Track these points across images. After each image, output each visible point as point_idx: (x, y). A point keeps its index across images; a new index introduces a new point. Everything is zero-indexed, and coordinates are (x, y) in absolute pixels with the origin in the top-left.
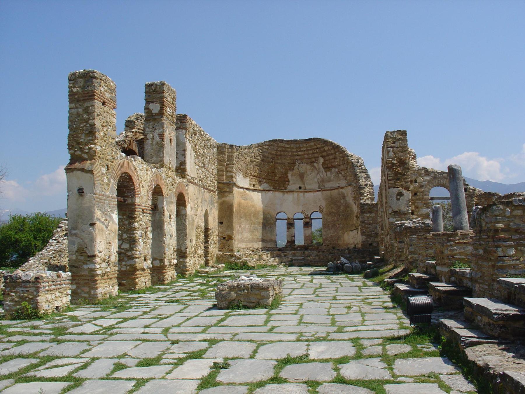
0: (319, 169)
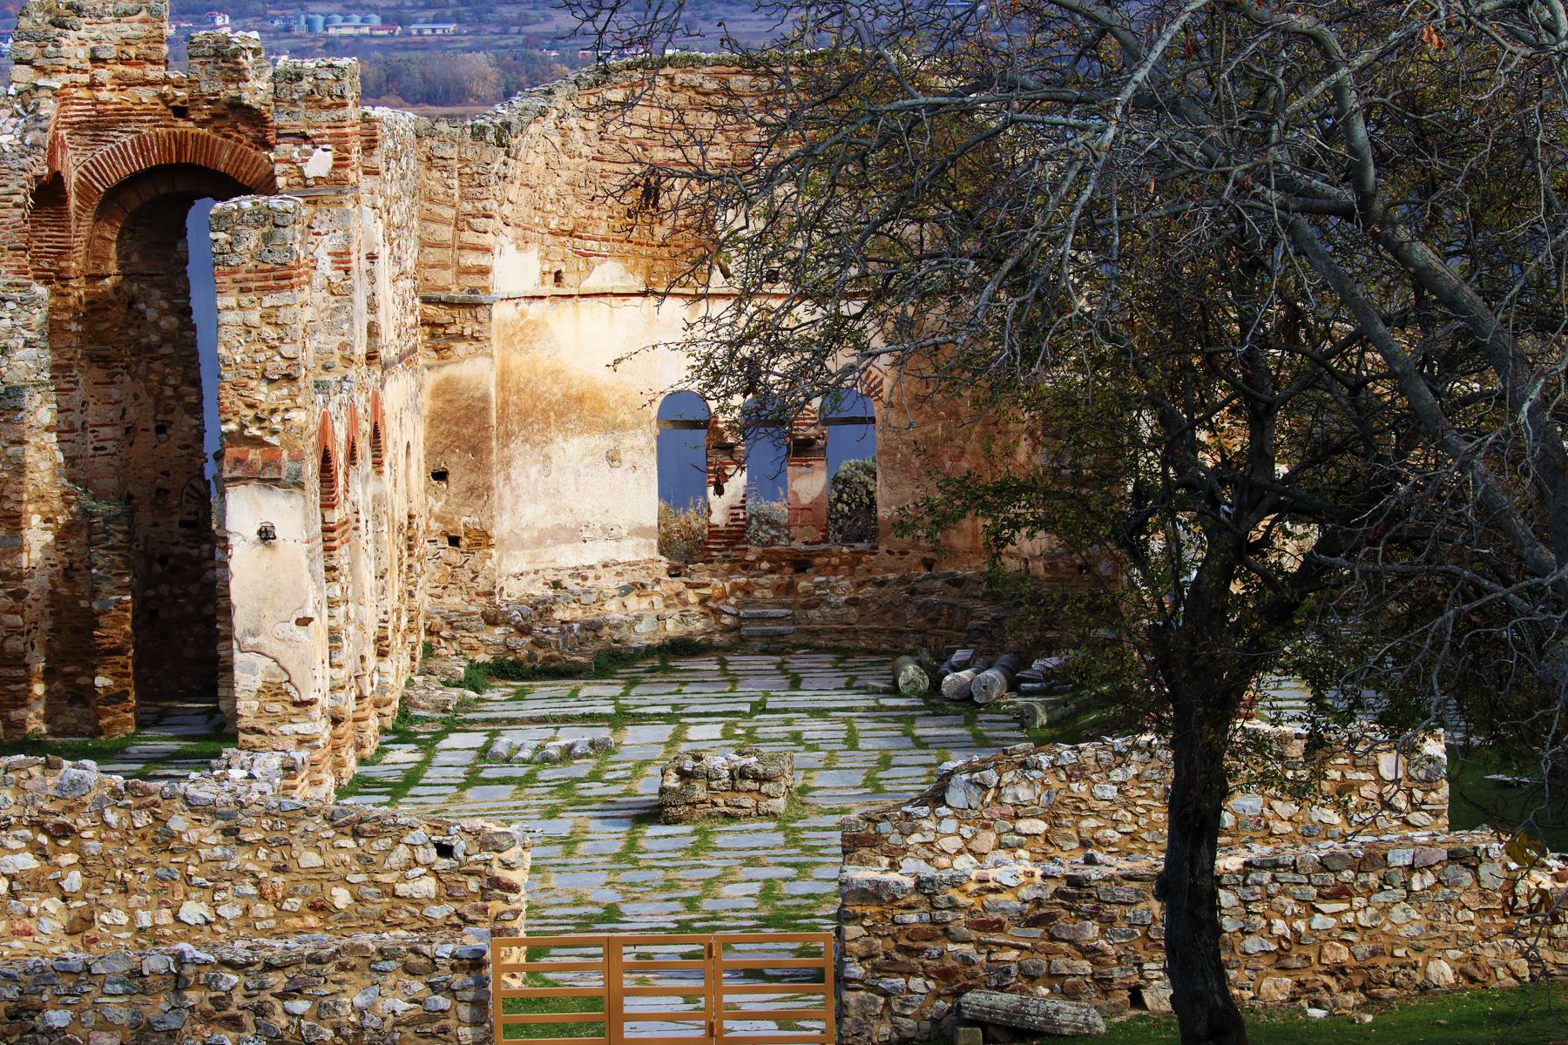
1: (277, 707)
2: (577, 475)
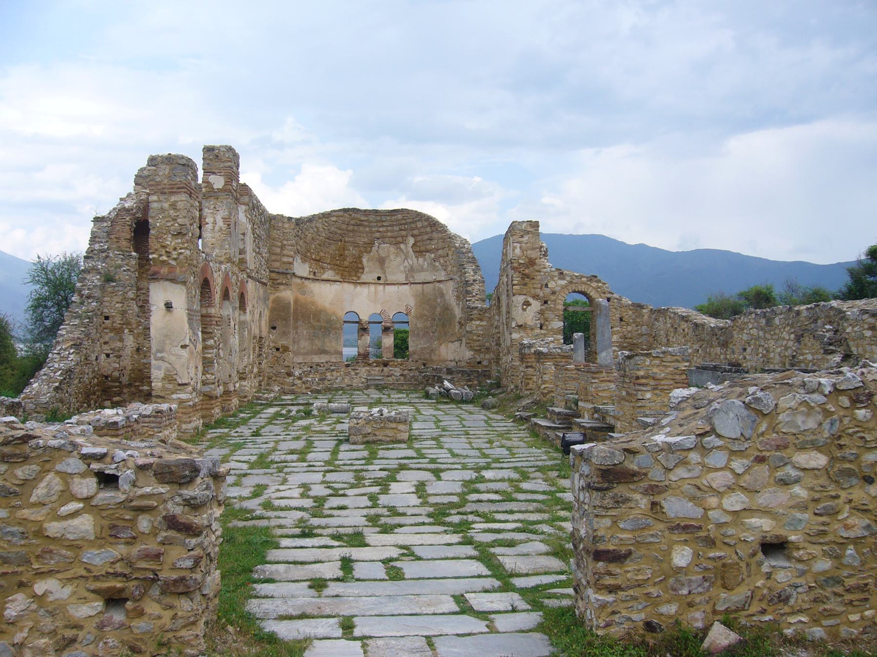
0: (408, 252)
1: (171, 386)
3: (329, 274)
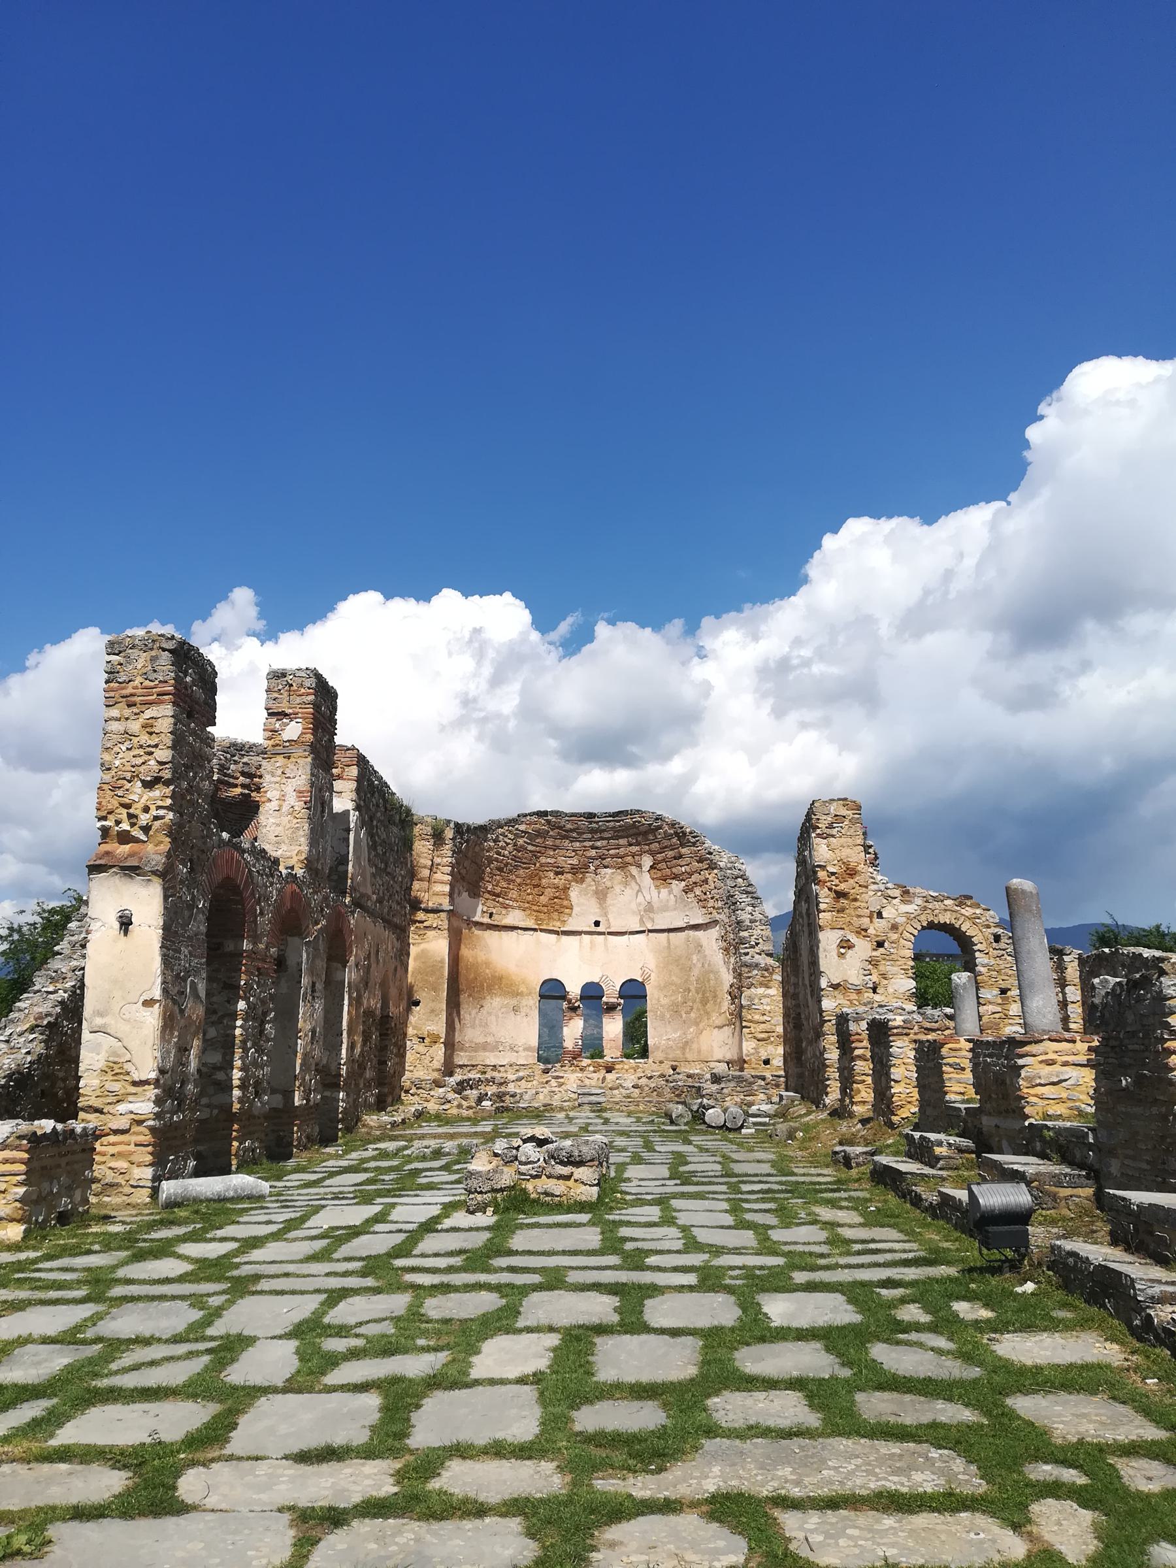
2: (497, 1017)
3: (514, 917)
